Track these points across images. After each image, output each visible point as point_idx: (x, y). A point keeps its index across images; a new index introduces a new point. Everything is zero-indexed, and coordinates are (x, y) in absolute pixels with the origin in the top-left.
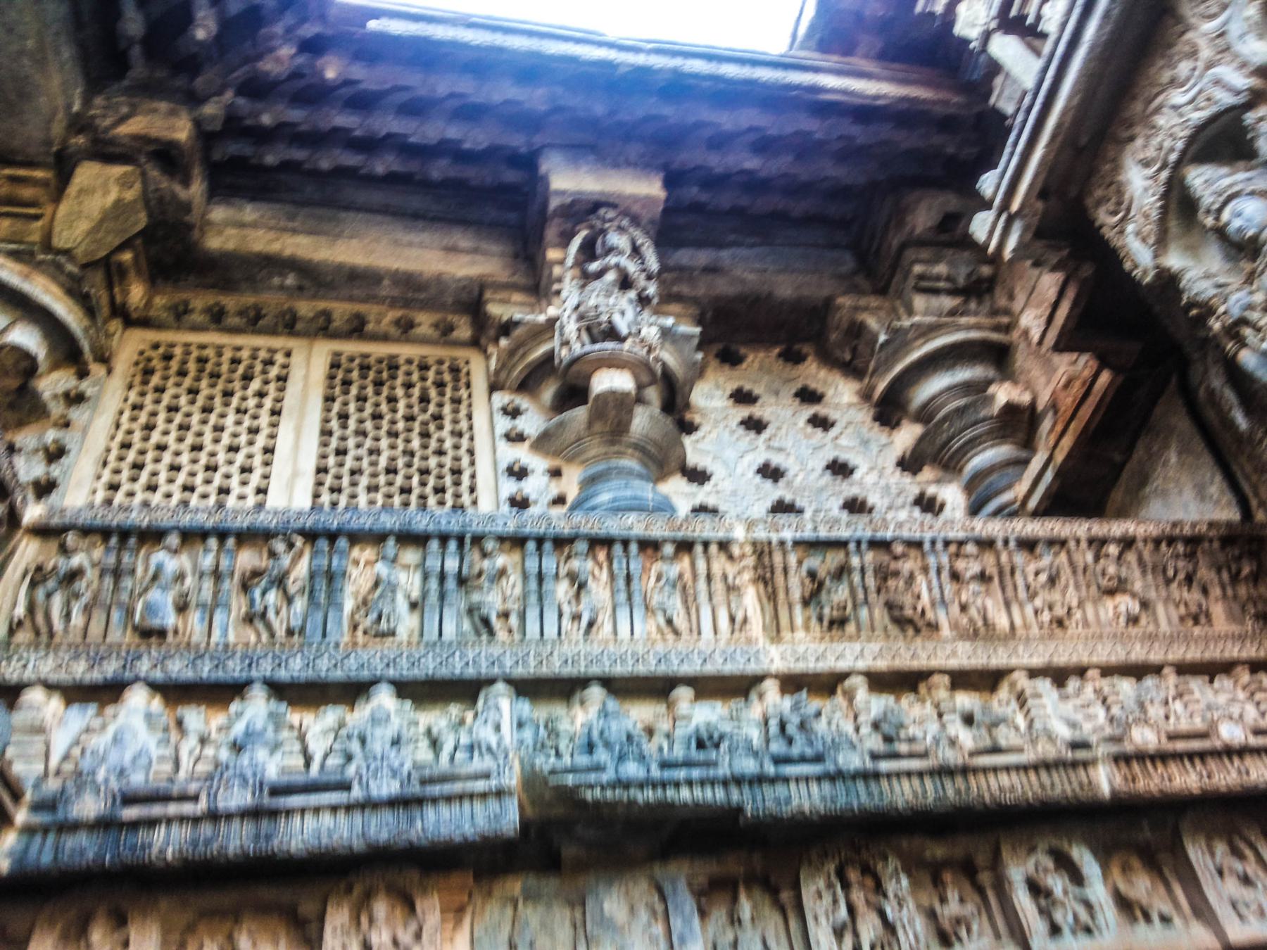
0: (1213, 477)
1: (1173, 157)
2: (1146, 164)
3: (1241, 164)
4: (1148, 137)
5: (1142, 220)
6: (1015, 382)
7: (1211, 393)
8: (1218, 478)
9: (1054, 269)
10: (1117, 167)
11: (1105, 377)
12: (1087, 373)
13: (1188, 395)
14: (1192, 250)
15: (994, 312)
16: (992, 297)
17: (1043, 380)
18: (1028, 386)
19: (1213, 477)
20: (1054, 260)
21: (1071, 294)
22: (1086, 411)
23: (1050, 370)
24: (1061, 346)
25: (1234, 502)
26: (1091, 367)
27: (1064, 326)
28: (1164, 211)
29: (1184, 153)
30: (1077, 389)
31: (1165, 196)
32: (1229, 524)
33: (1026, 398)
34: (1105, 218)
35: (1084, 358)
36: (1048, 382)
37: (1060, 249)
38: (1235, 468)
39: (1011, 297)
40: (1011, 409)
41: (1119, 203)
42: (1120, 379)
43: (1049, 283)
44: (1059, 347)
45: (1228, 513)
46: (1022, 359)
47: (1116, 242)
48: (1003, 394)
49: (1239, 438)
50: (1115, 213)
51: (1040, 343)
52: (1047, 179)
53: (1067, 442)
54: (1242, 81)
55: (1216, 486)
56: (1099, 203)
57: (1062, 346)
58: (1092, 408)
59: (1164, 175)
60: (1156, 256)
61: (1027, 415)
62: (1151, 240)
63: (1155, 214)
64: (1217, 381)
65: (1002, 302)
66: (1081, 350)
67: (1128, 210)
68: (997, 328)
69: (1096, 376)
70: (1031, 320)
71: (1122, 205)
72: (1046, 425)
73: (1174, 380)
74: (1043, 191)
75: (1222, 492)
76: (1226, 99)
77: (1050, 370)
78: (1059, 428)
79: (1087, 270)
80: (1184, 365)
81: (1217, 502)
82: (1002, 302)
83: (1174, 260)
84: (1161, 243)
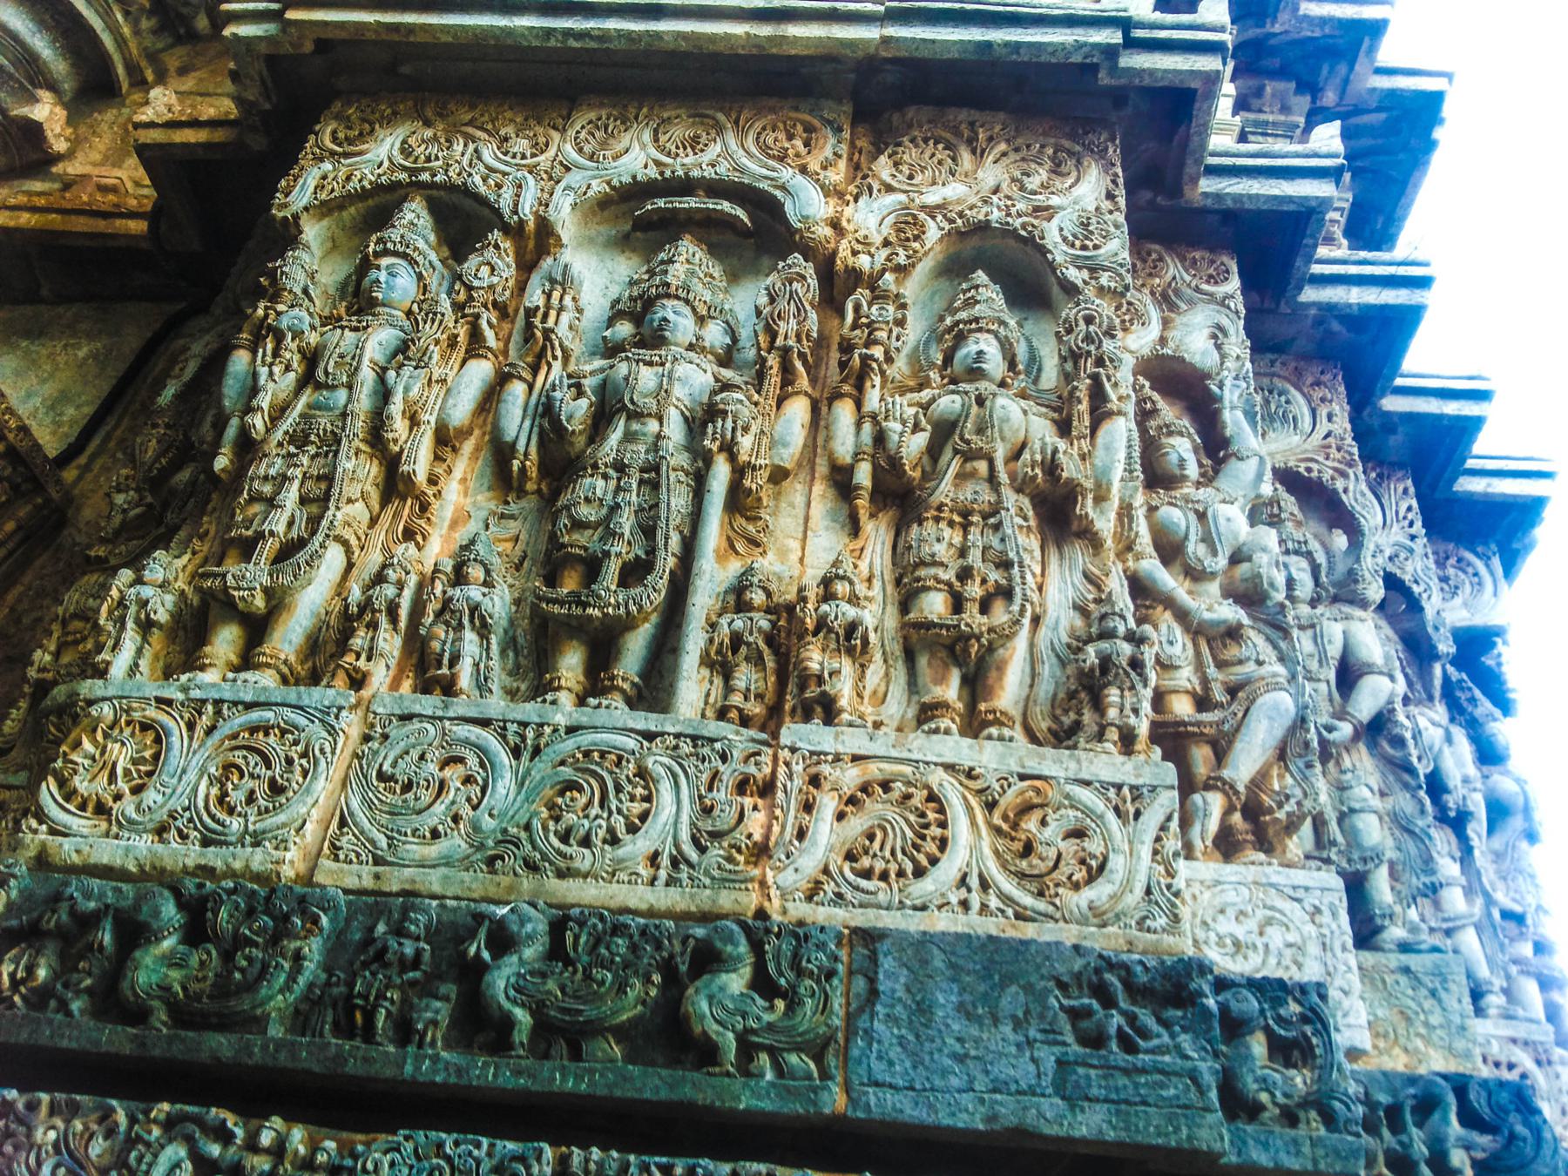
0: (87, 403)
1: (425, 177)
2: (406, 151)
3: (446, 252)
4: (435, 138)
5: (342, 175)
6: (70, 121)
7: (185, 349)
8: (88, 410)
9: (239, 100)
10: (390, 121)
11: (138, 226)
12: (133, 202)
13: (171, 328)
14: (333, 246)
15: (153, 57)
16: (172, 46)
17: (97, 157)
18: (76, 143)
19: (87, 403)
20: (251, 95)
21: (219, 136)
22: (81, 224)
23: (114, 158)
24: (147, 154)
25: (72, 439)
26: (140, 205)
27: (172, 145)
28: (363, 195)
29: (433, 185)
30: (107, 201)
31: (378, 188)
32: (37, 447)
33: (60, 146)
34: (326, 133)
35: (150, 192)
36: (95, 164)
37: (268, 98)
38: (111, 422)
39: (183, 71)
40: (34, 130)
41: (348, 139)
42: (144, 245)
43: (223, 106)
44: (143, 151)
45: (50, 442)
46: (108, 119)
47: (305, 158)
48: (45, 111)
49: (148, 410)
50: (335, 139)
51: (137, 126)
52: (344, 42)
53: (25, 219)
54: (527, 208)
55: (75, 414)
56: (338, 117)
57: (151, 157)
58: (85, 229)
59: (403, 176)
60: (306, 209)
61: (35, 156)
62: (323, 196)
63: (354, 185)
64: (199, 348)
65: (172, 61)
66: (155, 183)
67: (347, 155)
68: (132, 68)
69: (132, 215)
70: (161, 102)
71: (350, 145)
72: (38, 186)
73: (181, 306)
74: (328, 43)
75: (72, 422)
76: (505, 202)
77: (114, 158)
78: (42, 202)
79: (258, 142)
80: (201, 308)
81: (59, 424)
82: (172, 61)
83: (312, 232)
84: (324, 209)
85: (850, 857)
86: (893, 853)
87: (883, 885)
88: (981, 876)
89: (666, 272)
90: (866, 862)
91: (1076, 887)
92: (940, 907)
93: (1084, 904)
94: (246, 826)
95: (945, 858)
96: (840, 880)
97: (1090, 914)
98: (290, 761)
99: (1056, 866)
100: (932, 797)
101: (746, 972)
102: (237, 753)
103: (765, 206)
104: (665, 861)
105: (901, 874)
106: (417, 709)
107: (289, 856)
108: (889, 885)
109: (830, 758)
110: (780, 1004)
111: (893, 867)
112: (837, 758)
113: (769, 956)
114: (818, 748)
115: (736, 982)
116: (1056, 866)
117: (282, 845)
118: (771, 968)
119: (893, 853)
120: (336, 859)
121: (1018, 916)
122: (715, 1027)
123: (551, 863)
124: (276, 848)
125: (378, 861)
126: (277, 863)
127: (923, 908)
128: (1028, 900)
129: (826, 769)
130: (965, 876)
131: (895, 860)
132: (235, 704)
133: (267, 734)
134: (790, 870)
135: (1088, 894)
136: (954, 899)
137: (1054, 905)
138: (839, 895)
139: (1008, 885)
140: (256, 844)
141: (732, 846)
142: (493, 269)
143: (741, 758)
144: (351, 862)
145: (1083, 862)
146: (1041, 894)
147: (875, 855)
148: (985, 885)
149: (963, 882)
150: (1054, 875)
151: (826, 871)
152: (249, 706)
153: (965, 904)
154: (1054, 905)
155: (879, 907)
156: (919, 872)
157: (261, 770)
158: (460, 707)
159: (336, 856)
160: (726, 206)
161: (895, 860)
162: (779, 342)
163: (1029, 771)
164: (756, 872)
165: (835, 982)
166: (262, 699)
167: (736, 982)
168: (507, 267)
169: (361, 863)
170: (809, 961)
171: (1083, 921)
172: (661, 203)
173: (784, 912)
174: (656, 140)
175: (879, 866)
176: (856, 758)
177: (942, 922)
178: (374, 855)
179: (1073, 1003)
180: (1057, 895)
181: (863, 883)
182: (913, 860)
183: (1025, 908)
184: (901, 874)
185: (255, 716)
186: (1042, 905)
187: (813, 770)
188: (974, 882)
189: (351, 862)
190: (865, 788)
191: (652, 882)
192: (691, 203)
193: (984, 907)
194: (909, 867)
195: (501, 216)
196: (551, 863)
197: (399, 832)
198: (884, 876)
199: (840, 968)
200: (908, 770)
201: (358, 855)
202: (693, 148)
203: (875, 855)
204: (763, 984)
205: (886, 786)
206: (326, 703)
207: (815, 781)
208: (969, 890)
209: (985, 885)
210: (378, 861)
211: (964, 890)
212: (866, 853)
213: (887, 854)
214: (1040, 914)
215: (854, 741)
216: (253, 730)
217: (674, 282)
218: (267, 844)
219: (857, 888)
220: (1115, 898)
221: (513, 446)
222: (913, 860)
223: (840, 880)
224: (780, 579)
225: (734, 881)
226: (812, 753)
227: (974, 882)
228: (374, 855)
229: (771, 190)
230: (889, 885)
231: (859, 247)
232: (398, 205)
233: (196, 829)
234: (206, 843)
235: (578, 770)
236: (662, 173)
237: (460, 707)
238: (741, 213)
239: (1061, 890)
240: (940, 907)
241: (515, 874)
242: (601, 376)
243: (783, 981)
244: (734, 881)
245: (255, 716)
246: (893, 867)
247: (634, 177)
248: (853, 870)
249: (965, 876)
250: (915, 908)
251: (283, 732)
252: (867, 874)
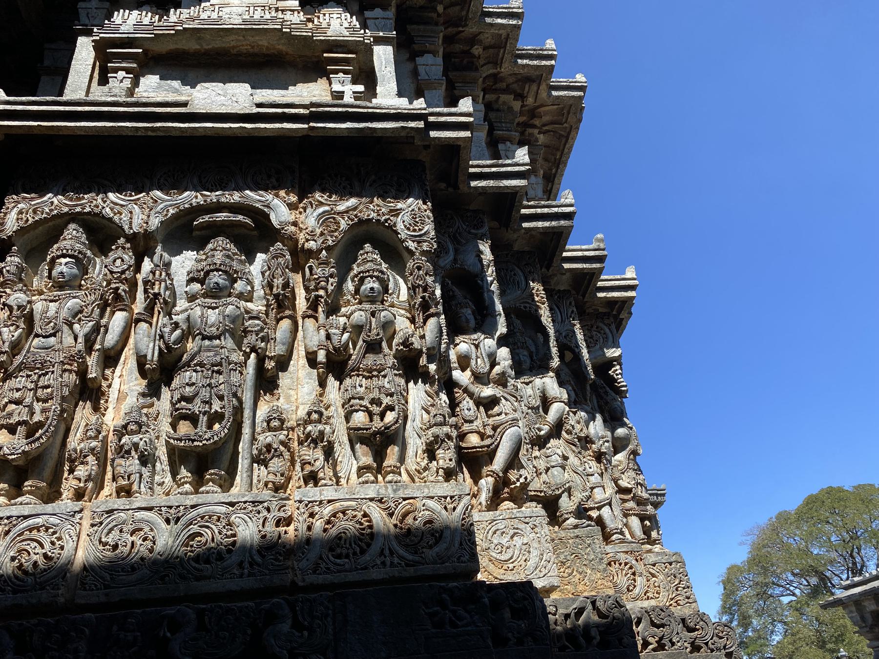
85: (331, 549)
86: (350, 545)
87: (347, 560)
88: (390, 549)
89: (214, 256)
90: (339, 551)
91: (431, 547)
92: (373, 567)
93: (434, 555)
94: (35, 580)
95: (373, 543)
96: (328, 561)
97: (437, 559)
98: (53, 543)
99: (422, 539)
100: (365, 515)
101: (289, 622)
102: (24, 543)
103: (260, 217)
104: (246, 565)
105: (355, 554)
106: (116, 507)
107: (60, 592)
108: (350, 560)
109: (318, 503)
110: (306, 633)
111: (351, 551)
112: (321, 502)
113: (299, 612)
114: (312, 499)
115: (285, 627)
116: (422, 539)
117: (56, 587)
118: (300, 618)
119: (350, 545)
120: (85, 589)
121: (407, 565)
122: (278, 649)
123: (192, 575)
124: (53, 589)
125: (106, 587)
126: (55, 596)
127: (366, 568)
128: (410, 557)
129: (316, 509)
130: (382, 550)
131: (352, 548)
132: (19, 517)
133: (39, 531)
134: (305, 560)
135: (436, 549)
136: (379, 563)
137: (422, 557)
138: (328, 569)
139: (402, 552)
140: (43, 589)
141: (277, 553)
142: (123, 261)
143: (277, 508)
144: (93, 590)
145: (433, 535)
146: (416, 553)
147: (342, 547)
148: (392, 553)
149: (382, 553)
150: (421, 544)
151: (321, 558)
152: (26, 517)
153: (384, 563)
154: (422, 557)
155: (346, 571)
156: (363, 552)
157: (39, 550)
158: (139, 501)
159: (85, 588)
160: (240, 217)
161: (352, 548)
162: (275, 289)
163: (407, 496)
164: (290, 563)
165: (329, 619)
166: (34, 513)
167: (285, 627)
168: (129, 258)
169: (98, 589)
170: (317, 612)
171: (435, 562)
172: (207, 218)
173: (304, 581)
174: (201, 182)
175: (344, 551)
176: (329, 501)
177: (375, 574)
178: (104, 584)
179: (431, 611)
180: (423, 552)
181: (338, 561)
182: (359, 546)
183: (409, 561)
184: (355, 554)
185: (31, 522)
186: (417, 558)
187: (311, 511)
188: (387, 552)
189: (93, 590)
190: (334, 515)
191: (241, 576)
192: (223, 216)
193: (392, 563)
194: (358, 550)
195: (123, 230)
196: (192, 575)
197: (116, 571)
198: (347, 556)
199: (330, 612)
200: (353, 503)
201: (96, 586)
202: (220, 186)
203: (342, 547)
204: (297, 625)
205: (344, 512)
206: (68, 510)
207: (312, 515)
208: (385, 557)
209: (392, 553)
210: (106, 587)
211: (383, 557)
212: (339, 547)
213: (348, 546)
214: (417, 562)
215: (329, 493)
216: (31, 530)
217: (218, 262)
218: (48, 588)
219: (336, 564)
220: (447, 549)
221: (145, 356)
222: (359, 546)
223: (328, 561)
224: (288, 412)
225: (280, 570)
226: (310, 502)
227: (387, 552)
228: (104, 584)
229: (262, 207)
230: (350, 560)
231: (309, 237)
232: (65, 226)
233: (8, 585)
234: (15, 592)
235: (200, 526)
236: (205, 201)
237: (139, 501)
238: (248, 221)
239: (424, 550)
240: (373, 567)
241: (176, 583)
242: (186, 314)
243: (306, 623)
244: (280, 570)
245: (31, 522)
246: (351, 551)
247: (191, 204)
248: (333, 555)
249: (382, 550)
250: (362, 569)
251: (47, 529)
252: (339, 556)
